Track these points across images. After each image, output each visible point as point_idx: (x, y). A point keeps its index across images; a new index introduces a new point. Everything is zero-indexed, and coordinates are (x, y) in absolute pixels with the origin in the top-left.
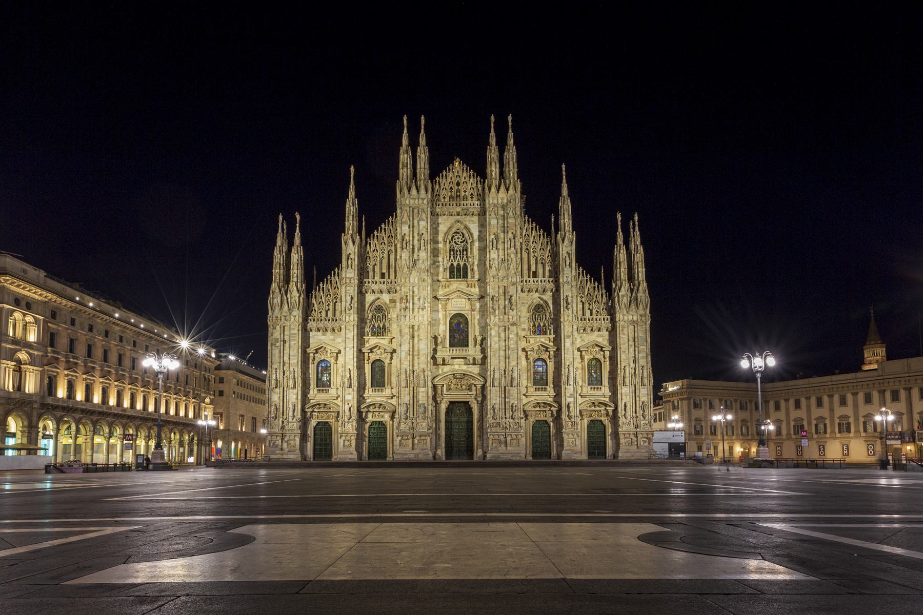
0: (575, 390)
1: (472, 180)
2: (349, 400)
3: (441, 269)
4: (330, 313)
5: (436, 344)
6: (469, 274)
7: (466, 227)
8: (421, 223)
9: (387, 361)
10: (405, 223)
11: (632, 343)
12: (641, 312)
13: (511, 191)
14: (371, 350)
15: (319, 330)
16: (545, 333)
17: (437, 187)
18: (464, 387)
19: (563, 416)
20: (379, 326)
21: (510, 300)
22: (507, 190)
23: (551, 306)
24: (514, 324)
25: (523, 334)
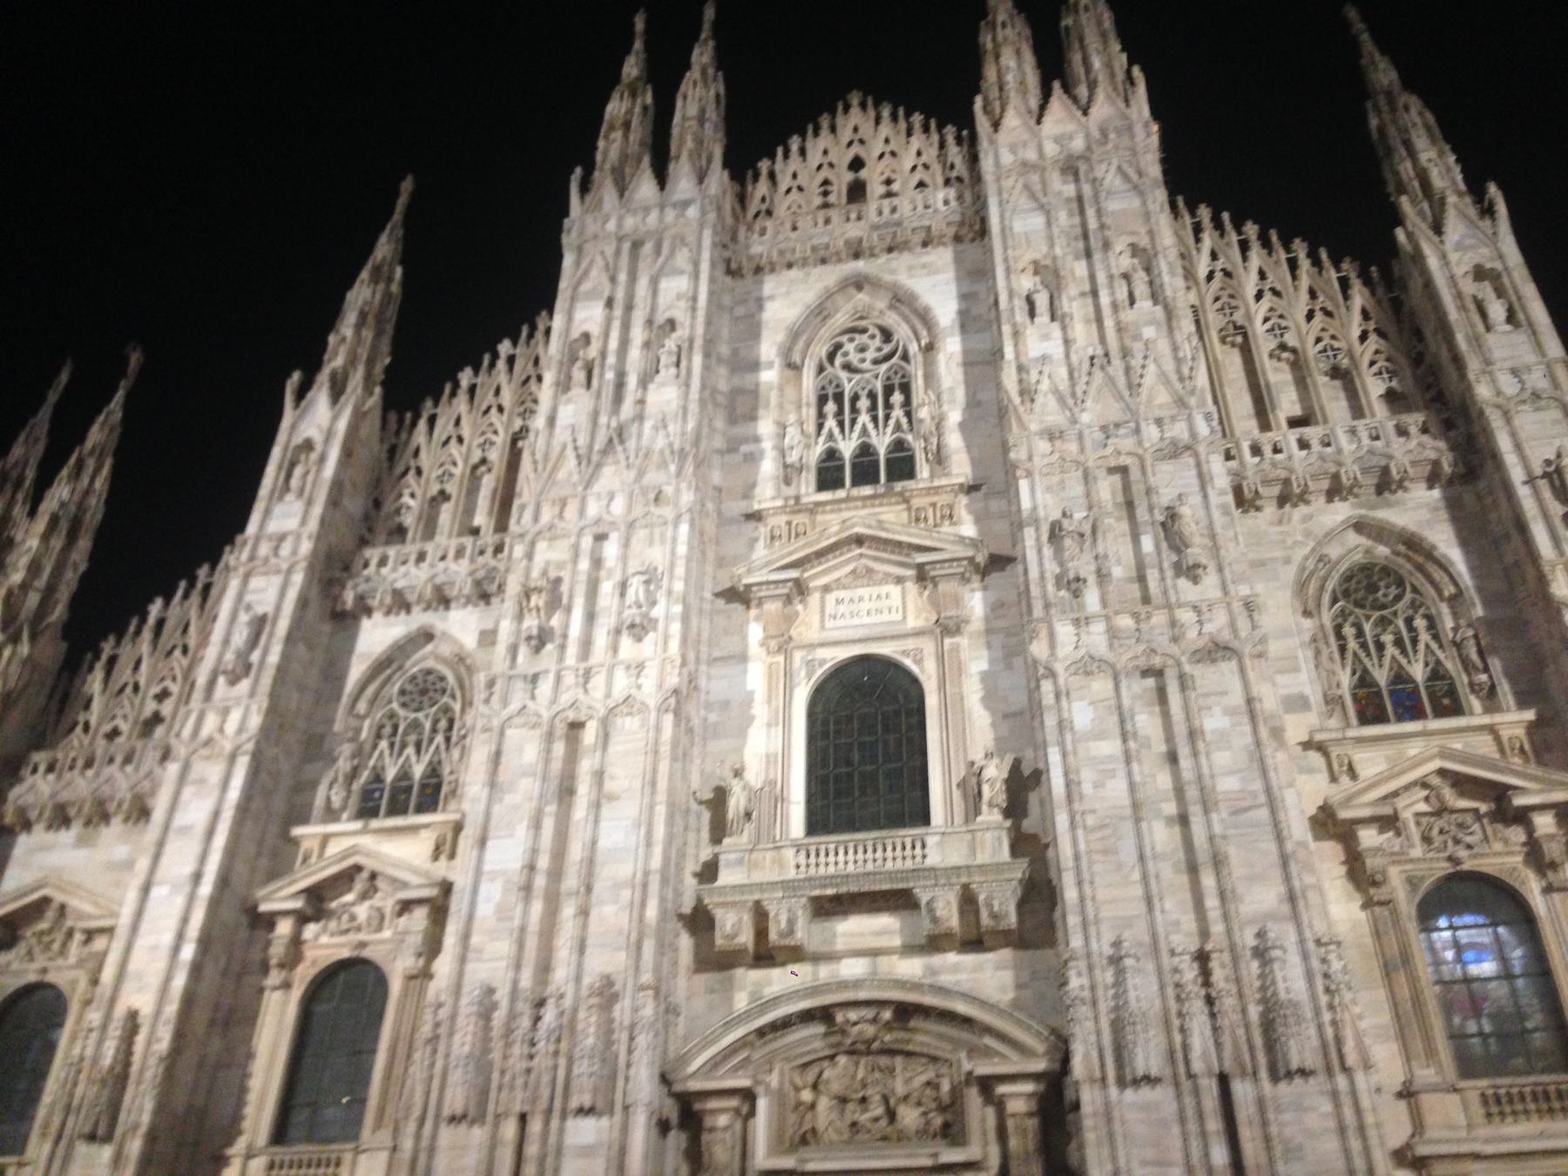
1: (917, 141)
3: (768, 467)
5: (719, 830)
7: (902, 300)
8: (664, 284)
9: (398, 970)
10: (592, 295)
13: (1102, 109)
14: (317, 903)
15: (61, 818)
17: (763, 187)
18: (909, 1117)
20: (404, 775)
23: (1454, 555)
24: (1216, 651)
25: (1297, 728)
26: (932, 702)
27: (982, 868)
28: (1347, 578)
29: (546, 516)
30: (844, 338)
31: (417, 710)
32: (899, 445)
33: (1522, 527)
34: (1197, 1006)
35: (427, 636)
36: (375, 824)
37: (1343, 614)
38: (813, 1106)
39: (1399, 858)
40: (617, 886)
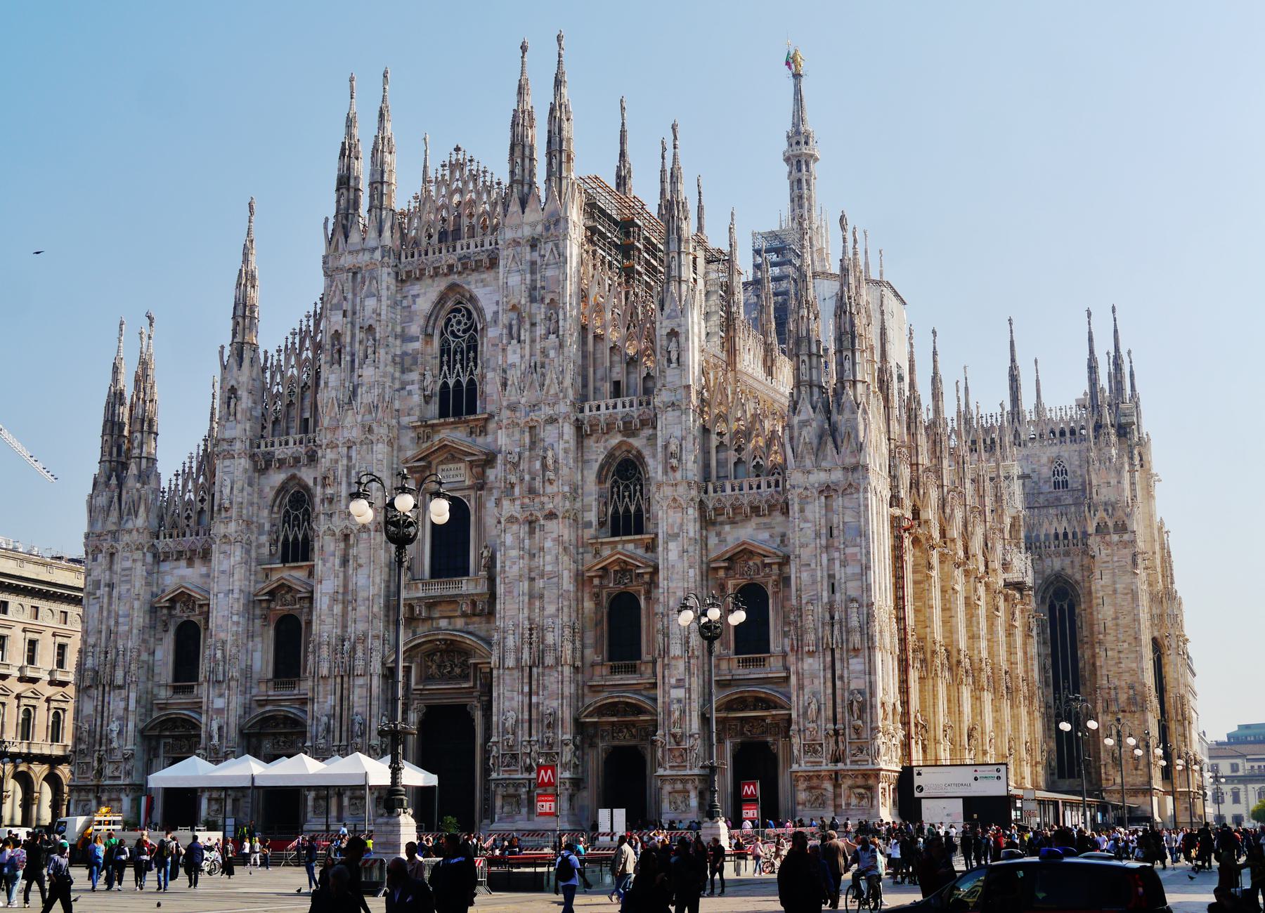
0: (688, 668)
2: (219, 711)
3: (417, 398)
4: (206, 517)
10: (337, 307)
16: (639, 531)
18: (457, 670)
20: (296, 538)
24: (551, 516)
26: (472, 518)
28: (620, 464)
29: (329, 437)
30: (451, 316)
32: (471, 382)
34: (526, 647)
35: (293, 477)
37: (615, 482)
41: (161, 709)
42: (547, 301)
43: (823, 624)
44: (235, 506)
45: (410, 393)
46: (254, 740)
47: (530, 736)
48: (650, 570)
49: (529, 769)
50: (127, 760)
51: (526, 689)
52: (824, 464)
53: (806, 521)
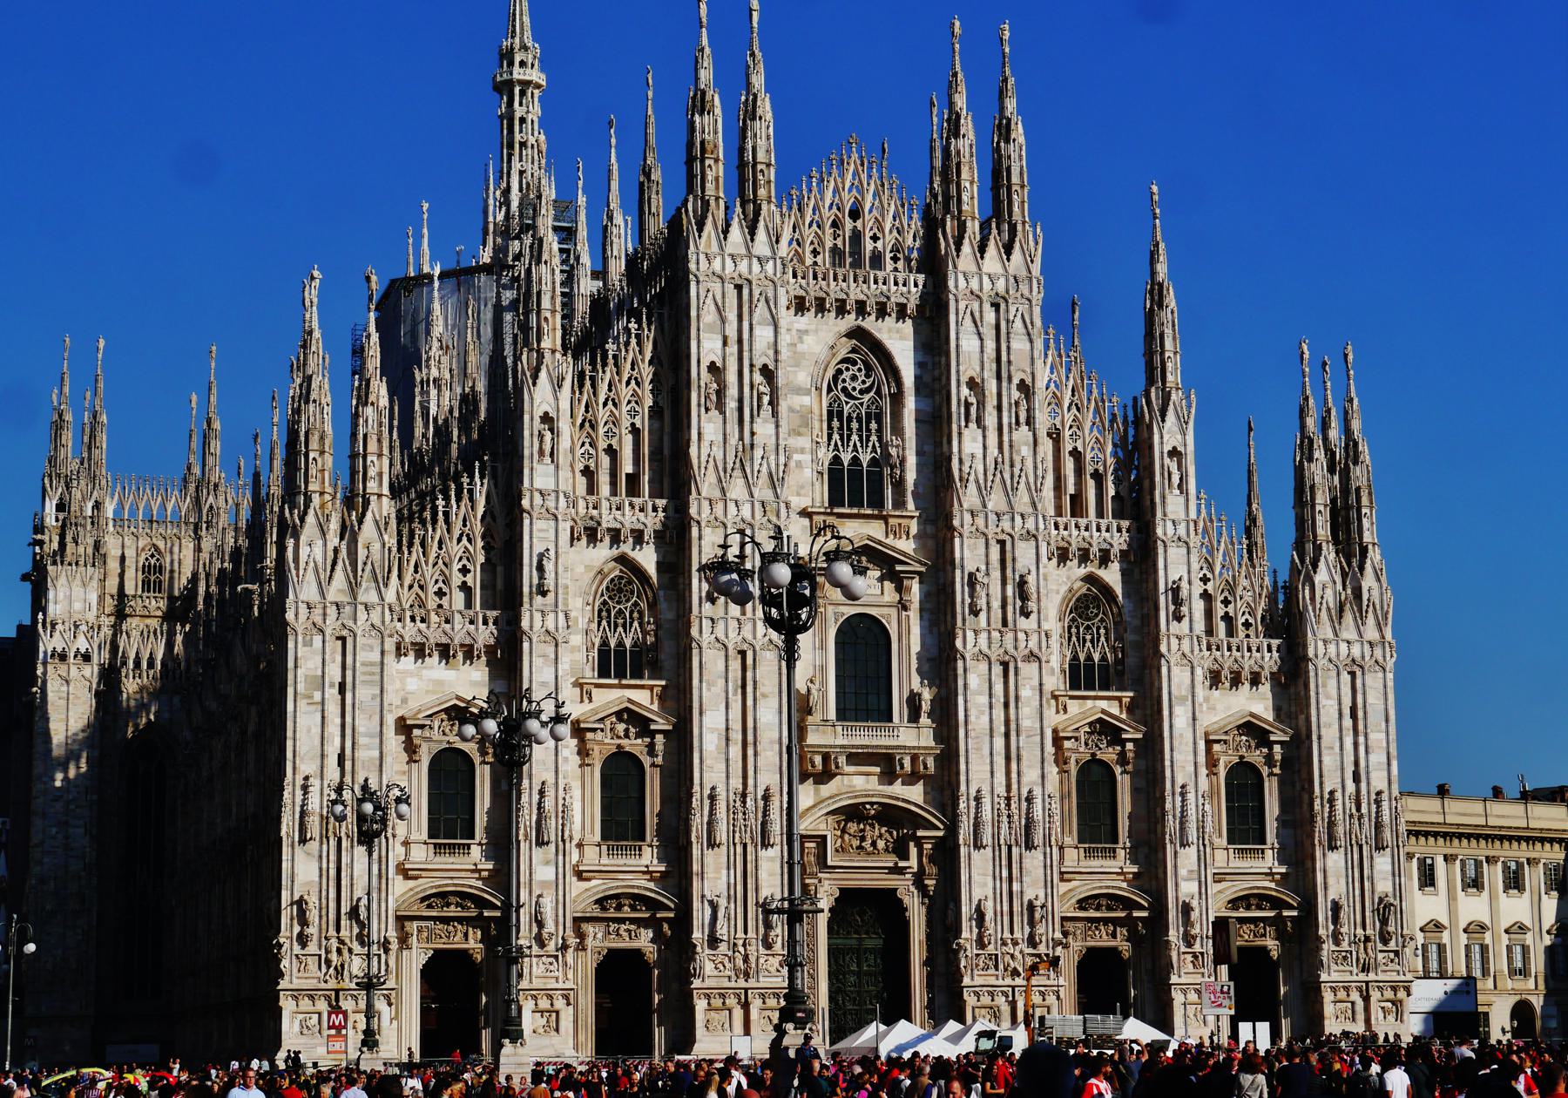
0: (1202, 859)
3: (808, 473)
6: (889, 492)
8: (757, 331)
11: (1348, 722)
12: (1371, 633)
13: (1017, 255)
18: (881, 844)
19: (1174, 935)
20: (620, 644)
21: (1022, 584)
22: (1008, 249)
24: (1032, 656)
27: (925, 748)
31: (619, 603)
32: (873, 462)
33: (1157, 609)
34: (1005, 819)
36: (624, 682)
37: (1073, 620)
38: (842, 837)
39: (1076, 751)
40: (772, 742)
41: (407, 877)
42: (1016, 381)
43: (1351, 816)
44: (560, 591)
45: (799, 464)
46: (584, 926)
47: (1012, 932)
48: (1140, 736)
49: (1015, 973)
50: (387, 951)
51: (1005, 873)
52: (1345, 635)
53: (1328, 697)
